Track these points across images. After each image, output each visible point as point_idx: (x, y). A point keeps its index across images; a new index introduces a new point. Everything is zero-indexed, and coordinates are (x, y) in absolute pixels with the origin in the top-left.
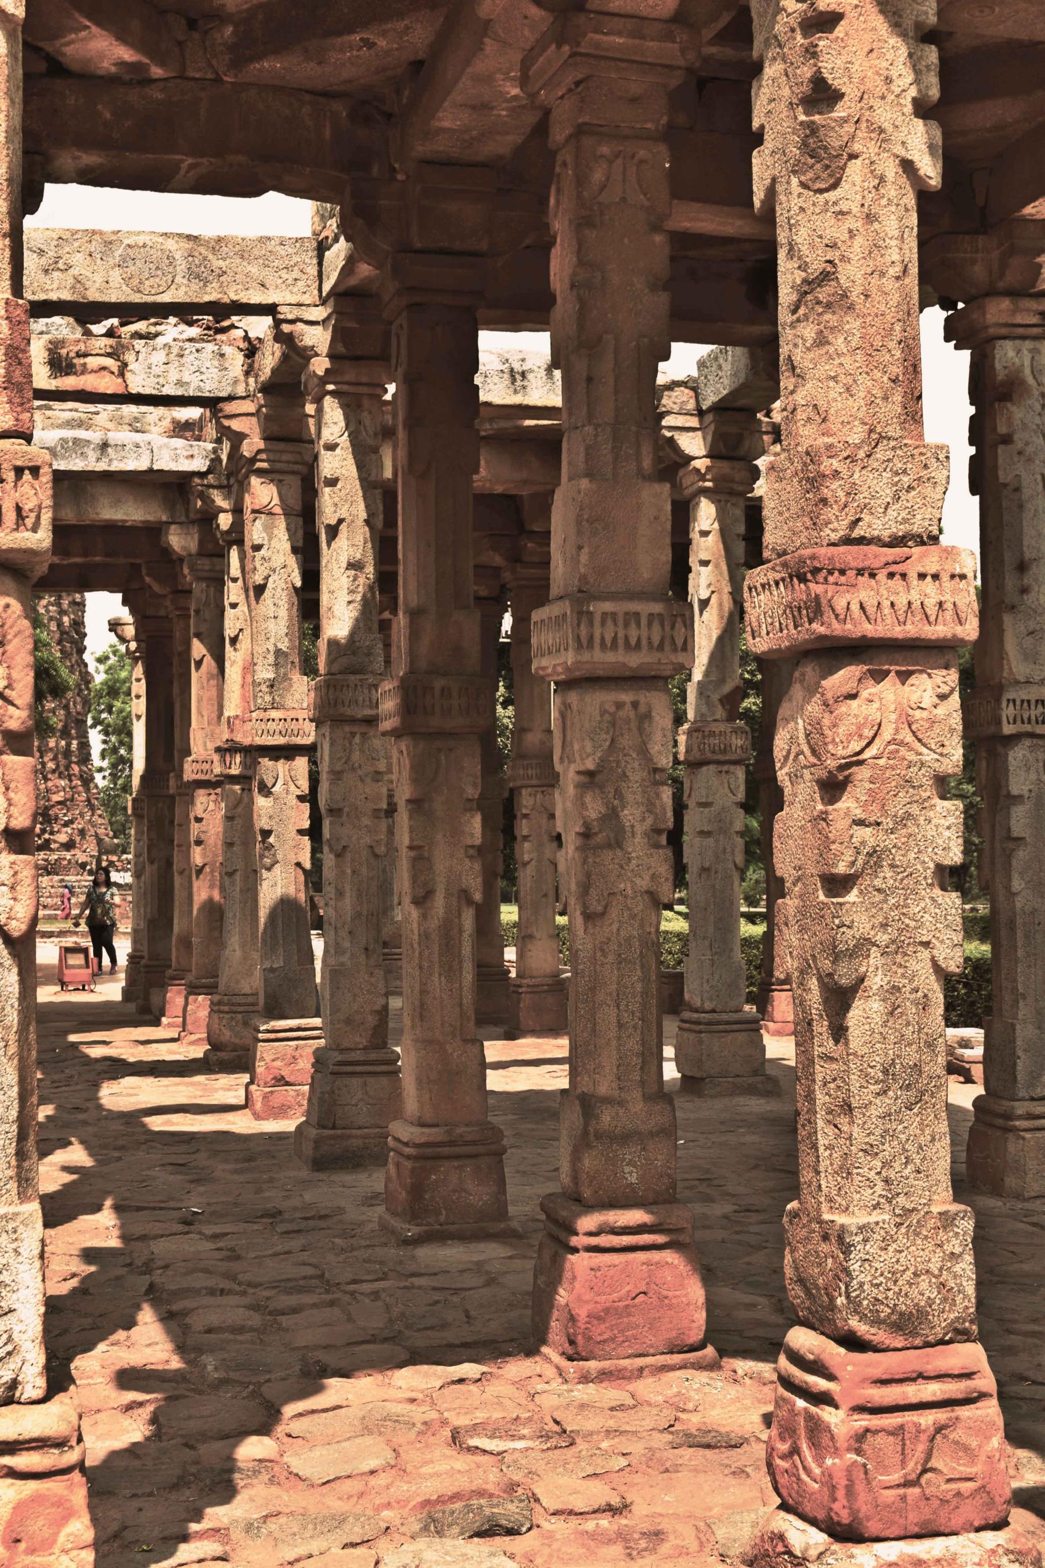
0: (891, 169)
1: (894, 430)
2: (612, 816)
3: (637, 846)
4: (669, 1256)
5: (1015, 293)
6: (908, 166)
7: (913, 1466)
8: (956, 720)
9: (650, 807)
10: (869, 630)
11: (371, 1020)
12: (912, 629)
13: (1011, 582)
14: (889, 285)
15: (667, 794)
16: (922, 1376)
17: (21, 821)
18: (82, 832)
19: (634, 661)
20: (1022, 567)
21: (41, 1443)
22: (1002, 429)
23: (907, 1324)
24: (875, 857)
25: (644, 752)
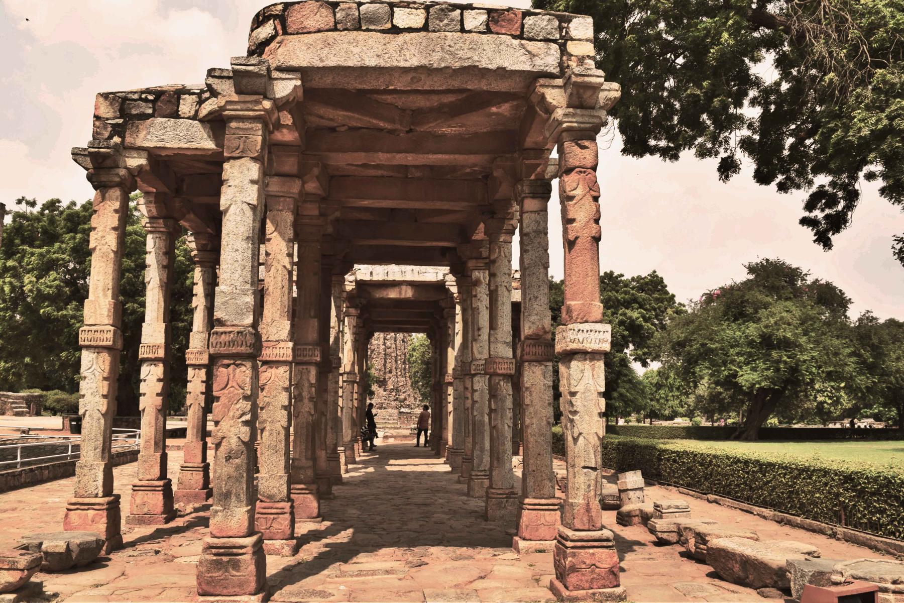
0: (280, 268)
1: (277, 319)
2: (300, 395)
3: (306, 401)
4: (309, 496)
5: (476, 258)
6: (284, 267)
7: (268, 525)
8: (288, 376)
9: (309, 392)
10: (268, 359)
11: (332, 446)
12: (277, 359)
13: (476, 333)
14: (278, 290)
15: (313, 389)
16: (272, 508)
17: (105, 393)
18: (409, 395)
19: (305, 359)
20: (479, 329)
21: (99, 504)
22: (474, 293)
23: (271, 497)
24: (268, 404)
25: (308, 380)
